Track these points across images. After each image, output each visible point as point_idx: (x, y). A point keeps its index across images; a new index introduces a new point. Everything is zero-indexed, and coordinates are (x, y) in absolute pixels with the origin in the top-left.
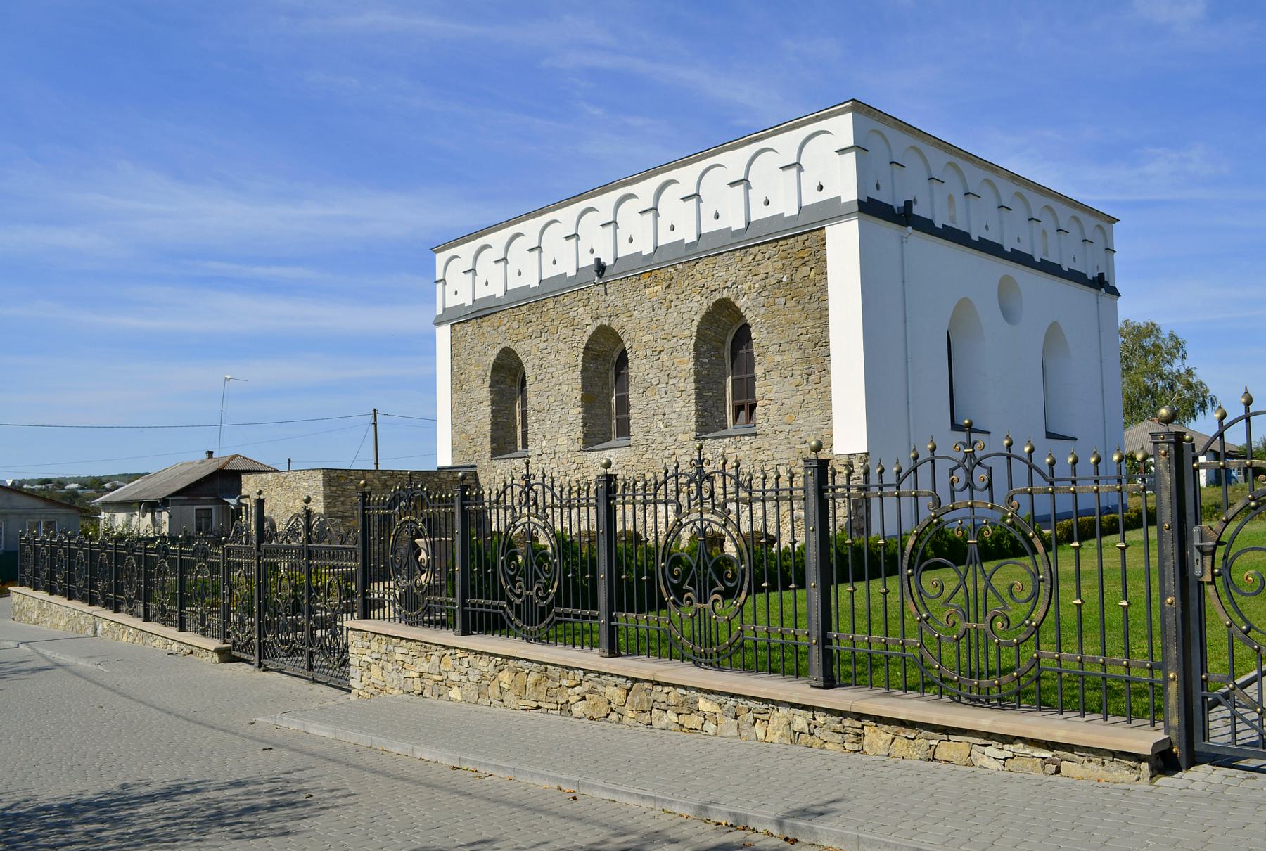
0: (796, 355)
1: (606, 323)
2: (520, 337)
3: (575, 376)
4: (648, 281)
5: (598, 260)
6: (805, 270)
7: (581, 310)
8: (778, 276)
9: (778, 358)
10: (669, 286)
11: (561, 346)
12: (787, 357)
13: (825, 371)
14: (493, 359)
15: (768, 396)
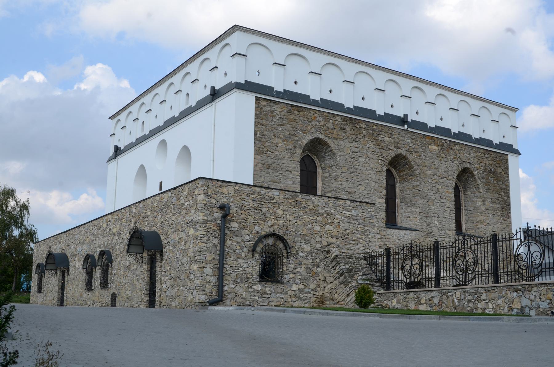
0: (498, 206)
1: (403, 152)
2: (334, 136)
3: (381, 178)
4: (431, 141)
5: (406, 116)
6: (499, 170)
7: (387, 139)
8: (491, 168)
9: (491, 205)
10: (441, 149)
11: (371, 155)
12: (494, 205)
13: (509, 217)
14: (305, 142)
15: (487, 221)
